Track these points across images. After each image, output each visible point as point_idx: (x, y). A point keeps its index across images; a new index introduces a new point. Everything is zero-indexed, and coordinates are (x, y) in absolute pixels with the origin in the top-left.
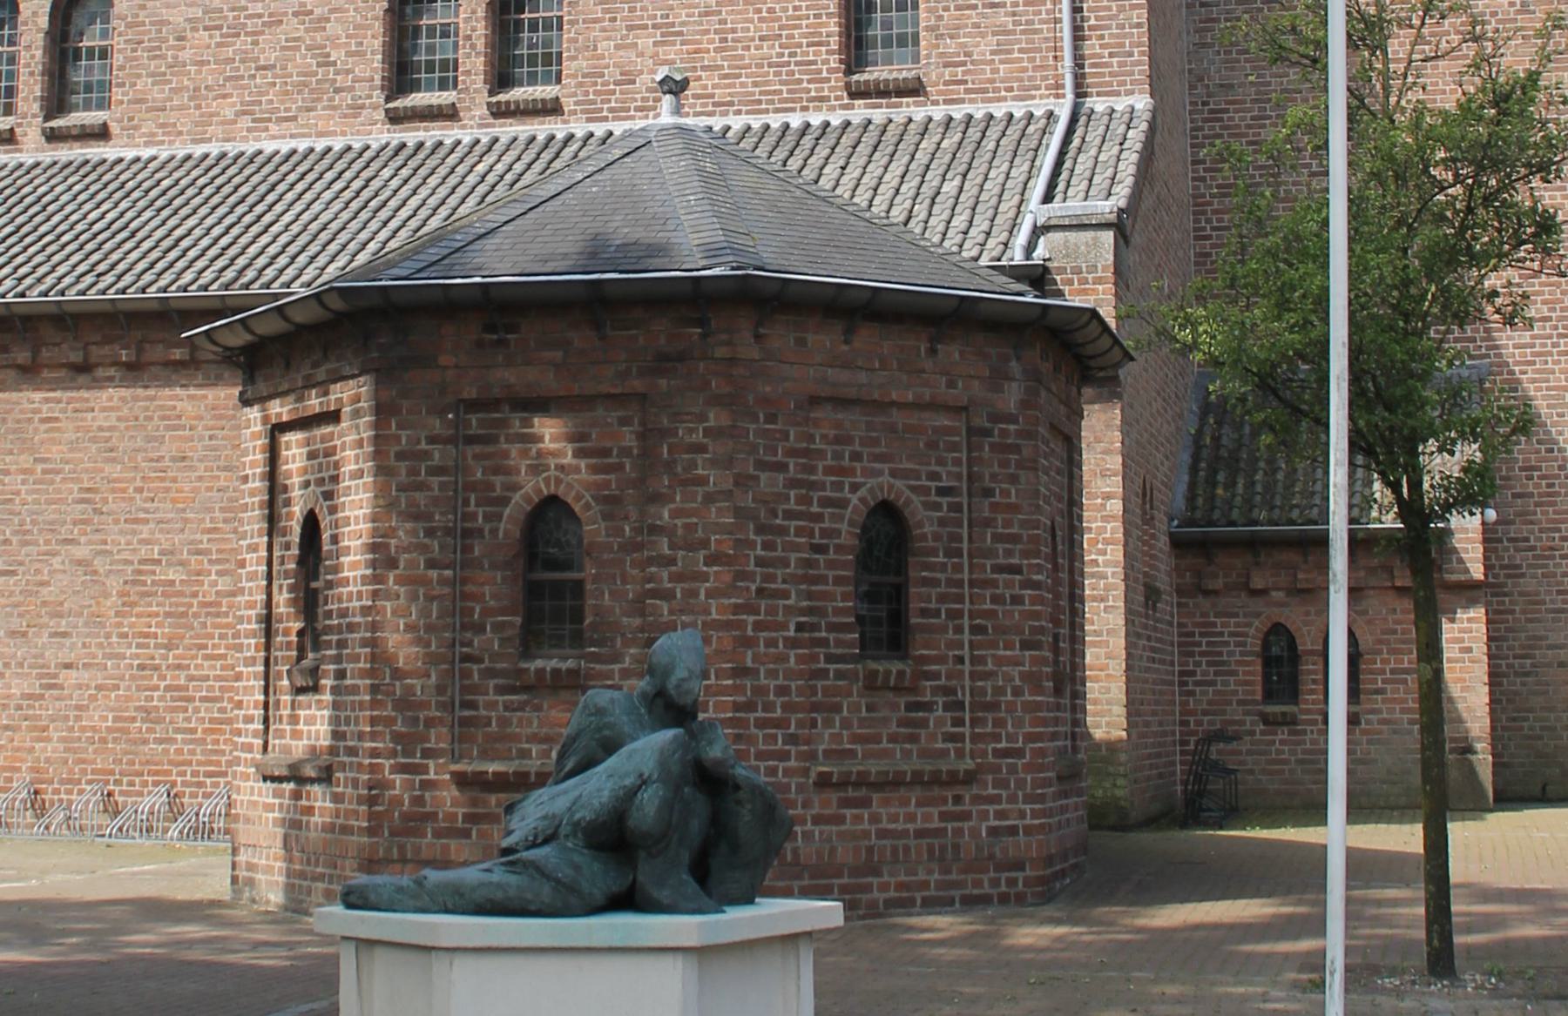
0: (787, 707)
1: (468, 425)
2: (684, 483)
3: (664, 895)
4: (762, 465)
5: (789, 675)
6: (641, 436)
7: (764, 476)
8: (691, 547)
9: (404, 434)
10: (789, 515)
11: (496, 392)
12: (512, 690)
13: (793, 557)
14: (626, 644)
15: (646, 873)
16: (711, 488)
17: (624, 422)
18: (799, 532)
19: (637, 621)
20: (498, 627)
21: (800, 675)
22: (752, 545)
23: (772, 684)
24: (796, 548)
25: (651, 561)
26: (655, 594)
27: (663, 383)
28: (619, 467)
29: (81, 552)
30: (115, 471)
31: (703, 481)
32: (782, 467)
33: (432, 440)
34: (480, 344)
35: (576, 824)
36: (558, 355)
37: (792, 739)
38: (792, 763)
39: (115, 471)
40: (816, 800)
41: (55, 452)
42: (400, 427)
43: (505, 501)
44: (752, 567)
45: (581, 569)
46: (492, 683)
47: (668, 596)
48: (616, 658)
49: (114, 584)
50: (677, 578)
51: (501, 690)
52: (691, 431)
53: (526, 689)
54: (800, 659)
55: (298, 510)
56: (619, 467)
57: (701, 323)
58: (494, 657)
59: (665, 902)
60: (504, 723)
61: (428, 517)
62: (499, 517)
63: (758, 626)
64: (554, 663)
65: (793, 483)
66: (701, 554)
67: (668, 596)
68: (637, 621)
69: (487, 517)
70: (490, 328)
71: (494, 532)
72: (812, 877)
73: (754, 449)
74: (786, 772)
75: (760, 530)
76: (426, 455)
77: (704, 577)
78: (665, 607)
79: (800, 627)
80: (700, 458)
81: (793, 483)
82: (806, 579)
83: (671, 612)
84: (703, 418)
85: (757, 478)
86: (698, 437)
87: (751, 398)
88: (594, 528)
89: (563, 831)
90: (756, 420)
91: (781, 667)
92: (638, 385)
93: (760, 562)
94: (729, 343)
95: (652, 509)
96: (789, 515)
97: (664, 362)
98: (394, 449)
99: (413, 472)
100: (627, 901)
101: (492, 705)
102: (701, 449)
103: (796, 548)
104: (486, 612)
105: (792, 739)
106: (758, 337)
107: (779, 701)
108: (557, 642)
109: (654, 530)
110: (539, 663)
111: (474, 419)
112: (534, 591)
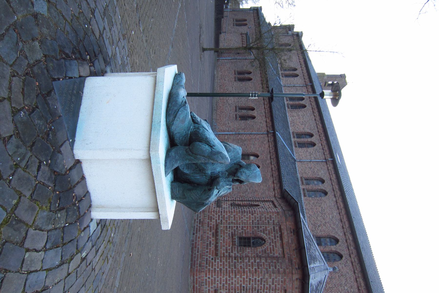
0: (229, 284)
1: (277, 227)
2: (269, 264)
3: (173, 153)
4: (273, 279)
5: (235, 284)
6: (277, 257)
7: (271, 280)
8: (258, 265)
9: (274, 216)
10: (264, 285)
11: (282, 231)
12: (232, 234)
13: (257, 286)
14: (240, 254)
15: (181, 150)
16: (269, 269)
17: (279, 254)
18: (261, 287)
19: (244, 256)
20: (242, 232)
21: (235, 287)
22: (259, 277)
23: (233, 281)
24: (258, 287)
25: (255, 258)
26: (249, 259)
27: (287, 261)
28: (271, 253)
29: (248, 190)
30: (260, 194)
31: (270, 268)
32: (273, 284)
33: (273, 221)
34: (291, 228)
35: (198, 128)
36: (290, 242)
37: (223, 285)
38: (219, 285)
39: (260, 194)
40: (213, 290)
41: (262, 187)
42: (275, 216)
43: (264, 233)
44: (255, 277)
45: (253, 246)
46: (233, 231)
47: (249, 261)
48: (238, 252)
49: (244, 195)
50: (252, 263)
51: (232, 232)
52: (279, 266)
53: (232, 237)
54: (238, 287)
55: (259, 204)
56: (271, 253)
57: (299, 268)
58: (237, 231)
59: (170, 153)
60: (227, 233)
61: (261, 220)
62: (261, 232)
63: (244, 278)
64: (237, 242)
65: (270, 286)
66: (257, 267)
67: (249, 261)
68: (244, 256)
69: (261, 230)
70: (293, 231)
71: (259, 231)
72: (199, 289)
73: (276, 278)
74: (218, 284)
75: (261, 279)
76: (271, 220)
77: (252, 268)
78: (247, 261)
79: (244, 287)
80: (274, 267)
81: (270, 286)
82: (252, 288)
83: (246, 262)
84: (281, 268)
85: (271, 278)
86: (277, 267)
87: (285, 277)
88: (260, 249)
89: (196, 125)
90: (282, 278)
91: (236, 283)
92: (286, 256)
93: (255, 279)
94: (295, 273)
95: (264, 259)
96: (264, 285)
97: (290, 261)
98: (271, 215)
99: (268, 218)
100: (172, 142)
101: (229, 231)
102: (276, 268)
103: (258, 287)
104: (245, 230)
105: (223, 285)
106: (297, 279)
107: (230, 282)
108: (240, 242)
109: (261, 259)
110: (237, 239)
111: (278, 228)
112: (249, 238)
